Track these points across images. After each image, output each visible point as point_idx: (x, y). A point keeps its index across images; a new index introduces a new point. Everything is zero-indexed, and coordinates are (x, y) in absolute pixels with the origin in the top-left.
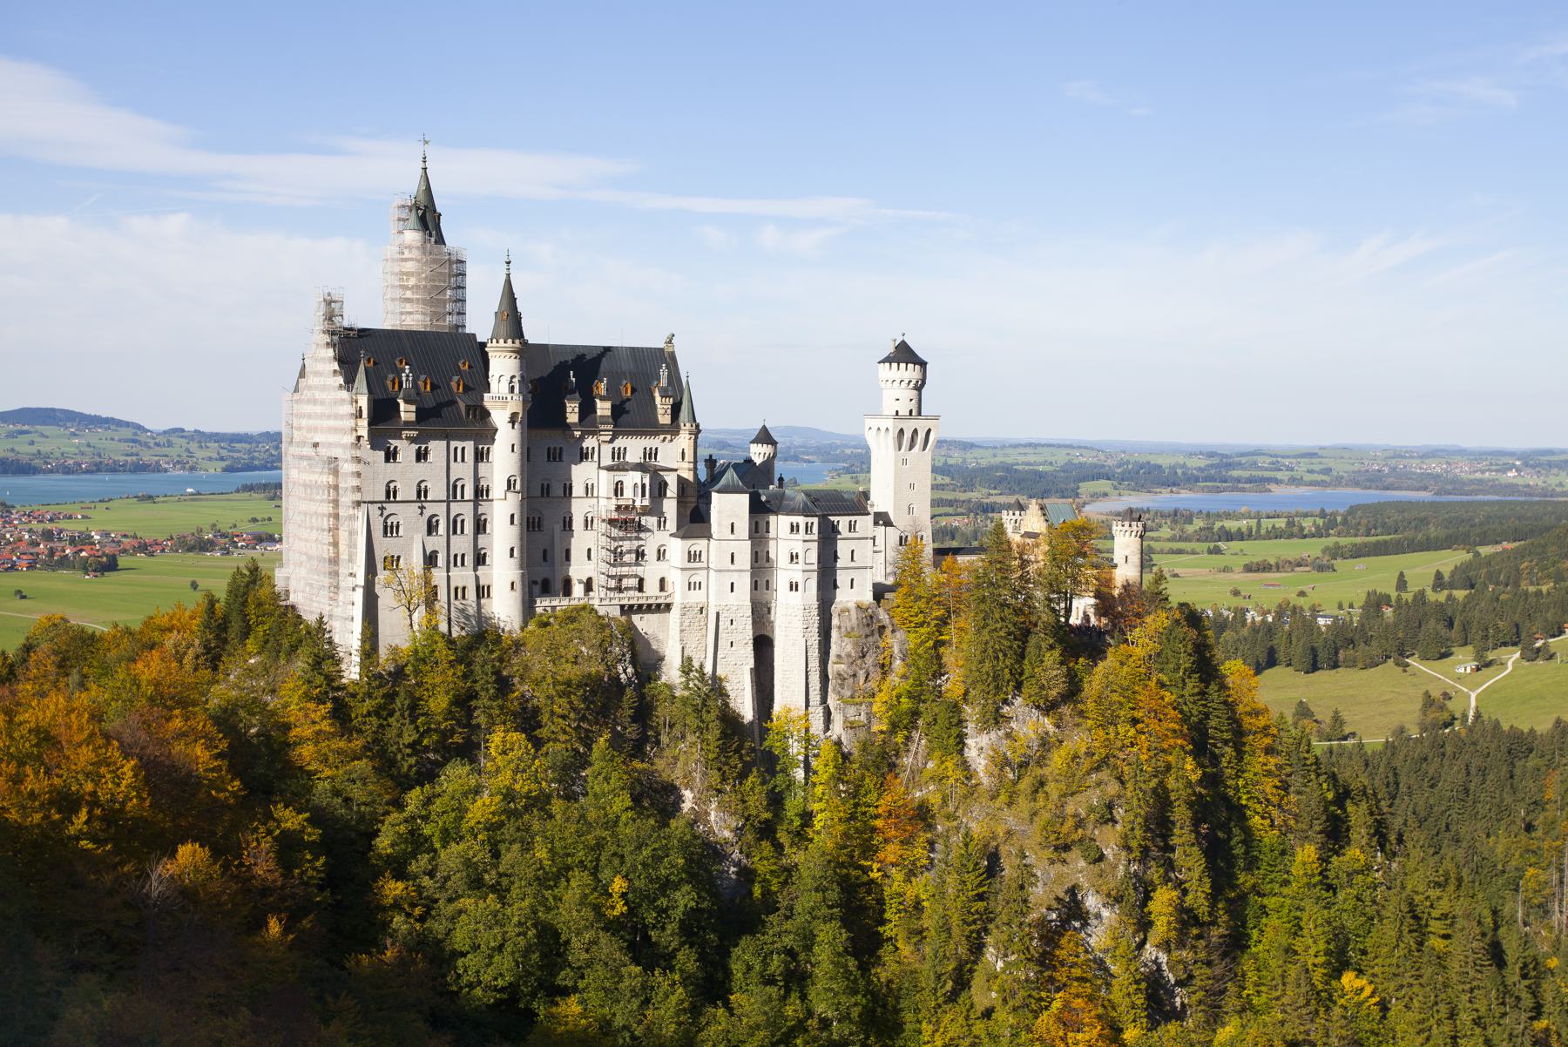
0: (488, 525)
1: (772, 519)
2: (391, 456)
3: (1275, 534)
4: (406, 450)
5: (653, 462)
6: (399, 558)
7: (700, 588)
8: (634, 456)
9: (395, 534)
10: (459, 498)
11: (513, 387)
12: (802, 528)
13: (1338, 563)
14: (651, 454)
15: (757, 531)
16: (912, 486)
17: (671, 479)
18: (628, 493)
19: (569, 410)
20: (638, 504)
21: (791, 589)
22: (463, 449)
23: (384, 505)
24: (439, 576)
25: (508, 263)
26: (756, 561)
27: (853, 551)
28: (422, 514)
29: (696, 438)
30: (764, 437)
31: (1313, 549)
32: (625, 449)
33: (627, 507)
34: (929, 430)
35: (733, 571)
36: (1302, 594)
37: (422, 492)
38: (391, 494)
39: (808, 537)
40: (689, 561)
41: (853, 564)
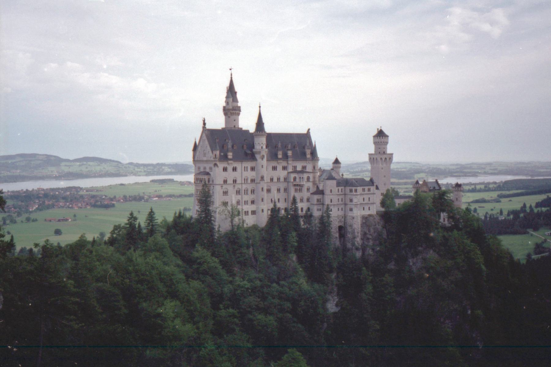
0: (255, 192)
1: (343, 188)
2: (225, 169)
3: (480, 191)
4: (230, 168)
5: (305, 170)
6: (227, 202)
7: (321, 210)
8: (299, 168)
9: (226, 195)
10: (246, 182)
11: (262, 147)
12: (354, 190)
13: (503, 200)
14: (304, 167)
15: (338, 192)
16: (385, 176)
17: (311, 176)
18: (297, 180)
19: (279, 154)
20: (300, 184)
21: (350, 211)
22: (247, 167)
23: (224, 185)
24: (239, 207)
25: (260, 107)
26: (338, 202)
27: (369, 198)
28: (234, 188)
29: (318, 162)
30: (337, 162)
31: (494, 195)
32: (296, 166)
33: (297, 185)
34: (390, 158)
35: (331, 205)
36: (492, 210)
37: (235, 181)
38: (225, 182)
39: (355, 194)
40: (317, 202)
41: (369, 202)
